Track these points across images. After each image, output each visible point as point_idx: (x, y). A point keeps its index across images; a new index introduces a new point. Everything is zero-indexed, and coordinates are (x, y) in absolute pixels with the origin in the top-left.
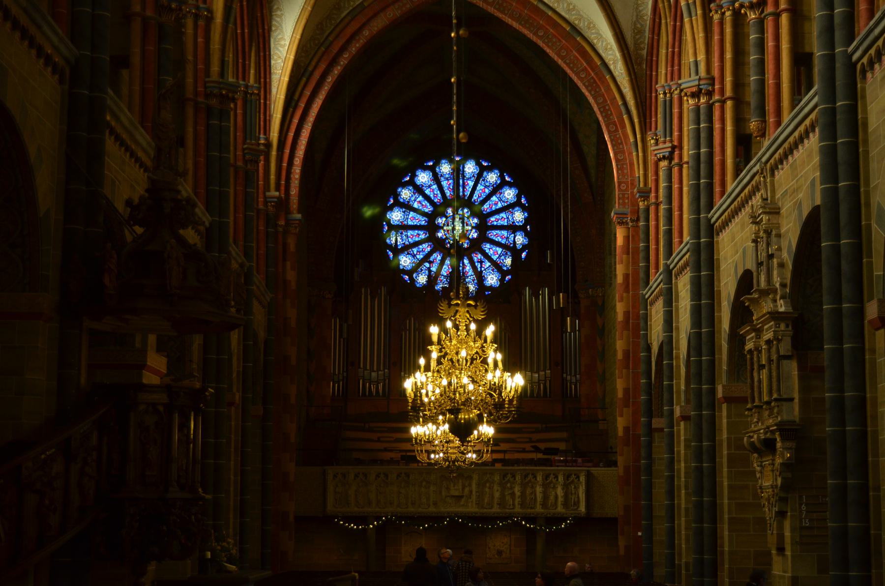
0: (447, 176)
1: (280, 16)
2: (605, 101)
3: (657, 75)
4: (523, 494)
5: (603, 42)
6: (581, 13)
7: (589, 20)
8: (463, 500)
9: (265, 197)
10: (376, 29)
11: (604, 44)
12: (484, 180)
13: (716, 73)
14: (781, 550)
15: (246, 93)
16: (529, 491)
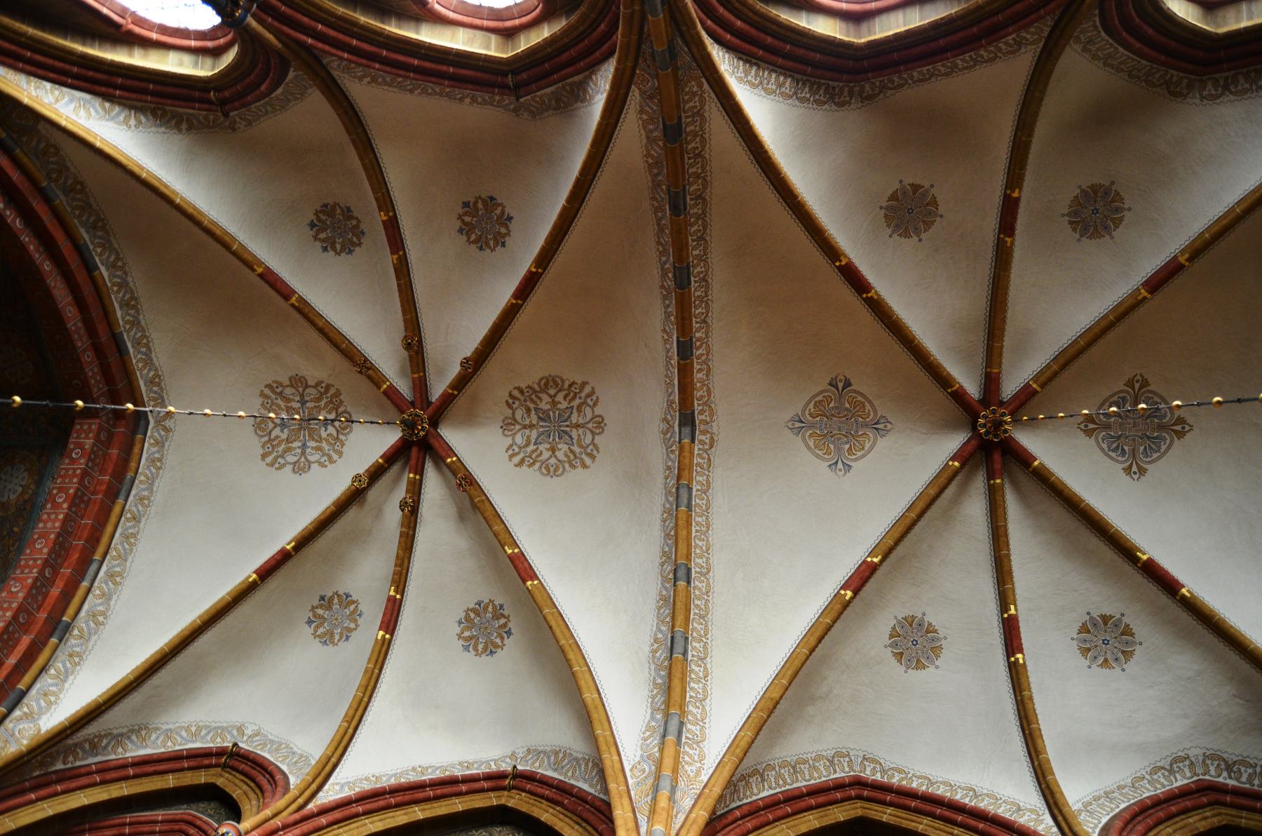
1: (126, 122)
3: (31, 802)
5: (56, 685)
6: (94, 638)
7: (84, 653)
10: (53, 284)
11: (54, 689)
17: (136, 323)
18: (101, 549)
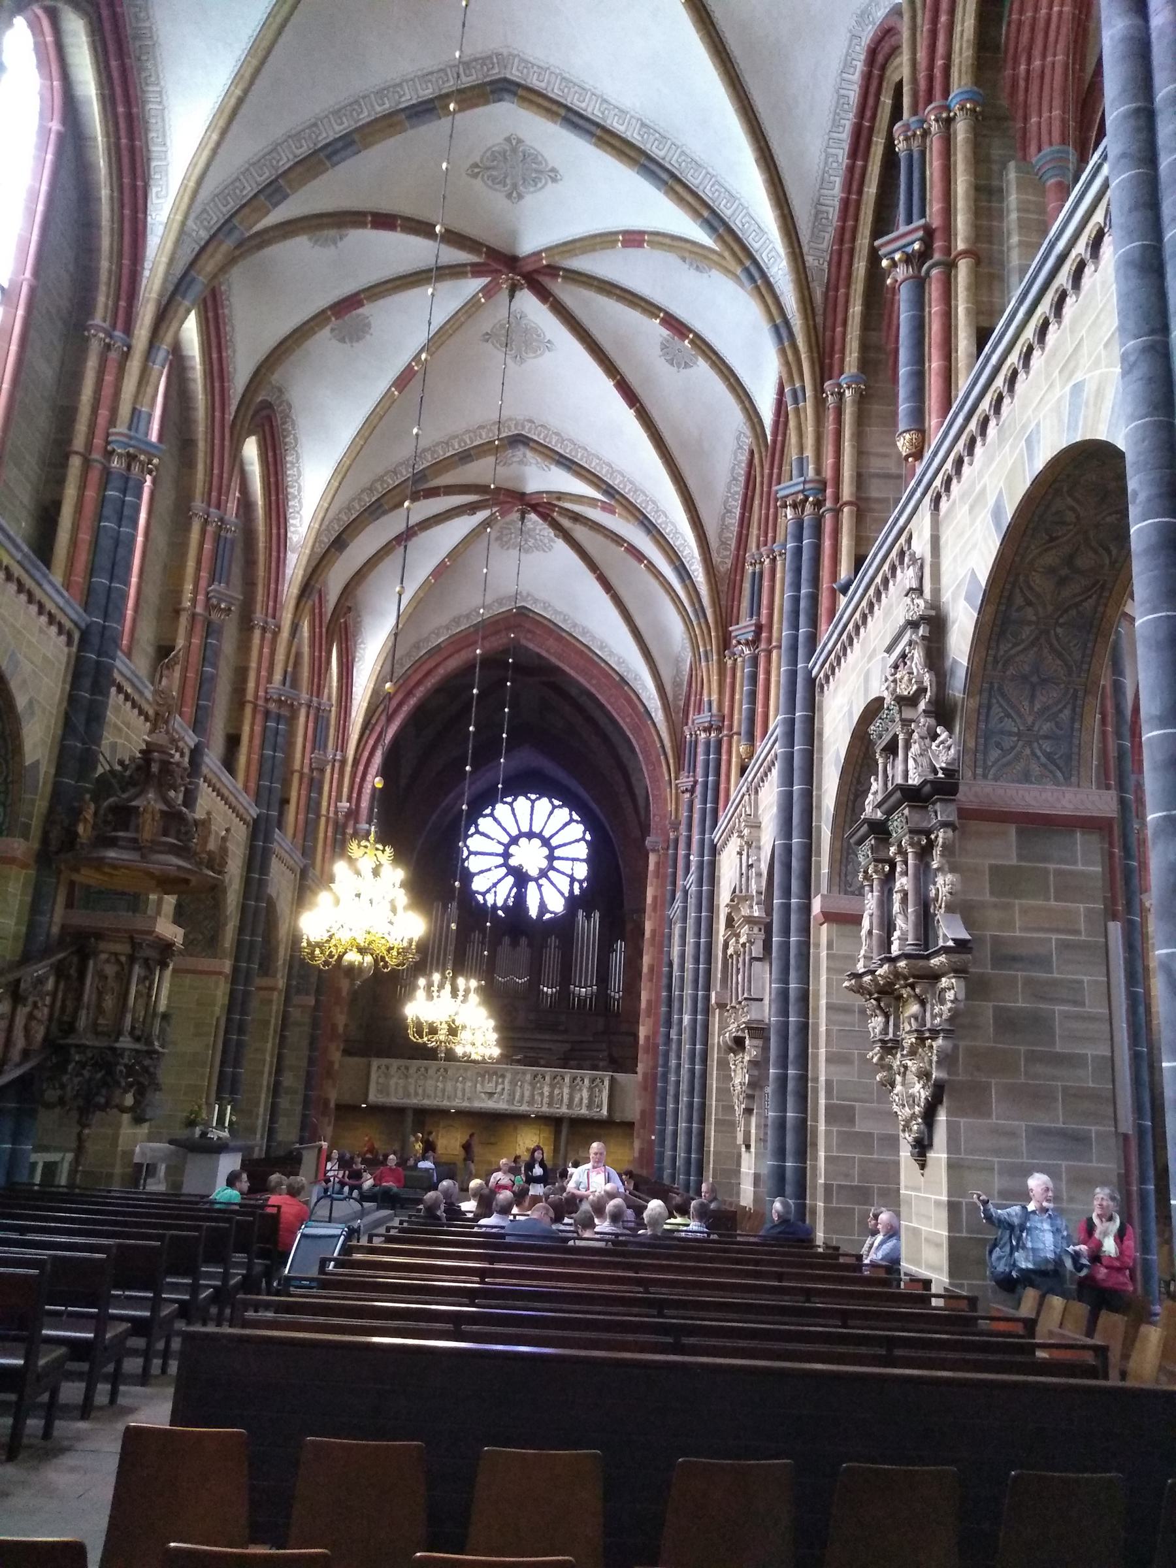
2: (646, 743)
9: (336, 807)
13: (726, 711)
14: (748, 1147)
15: (318, 709)
16: (556, 1092)
17: (468, 616)
18: (586, 651)
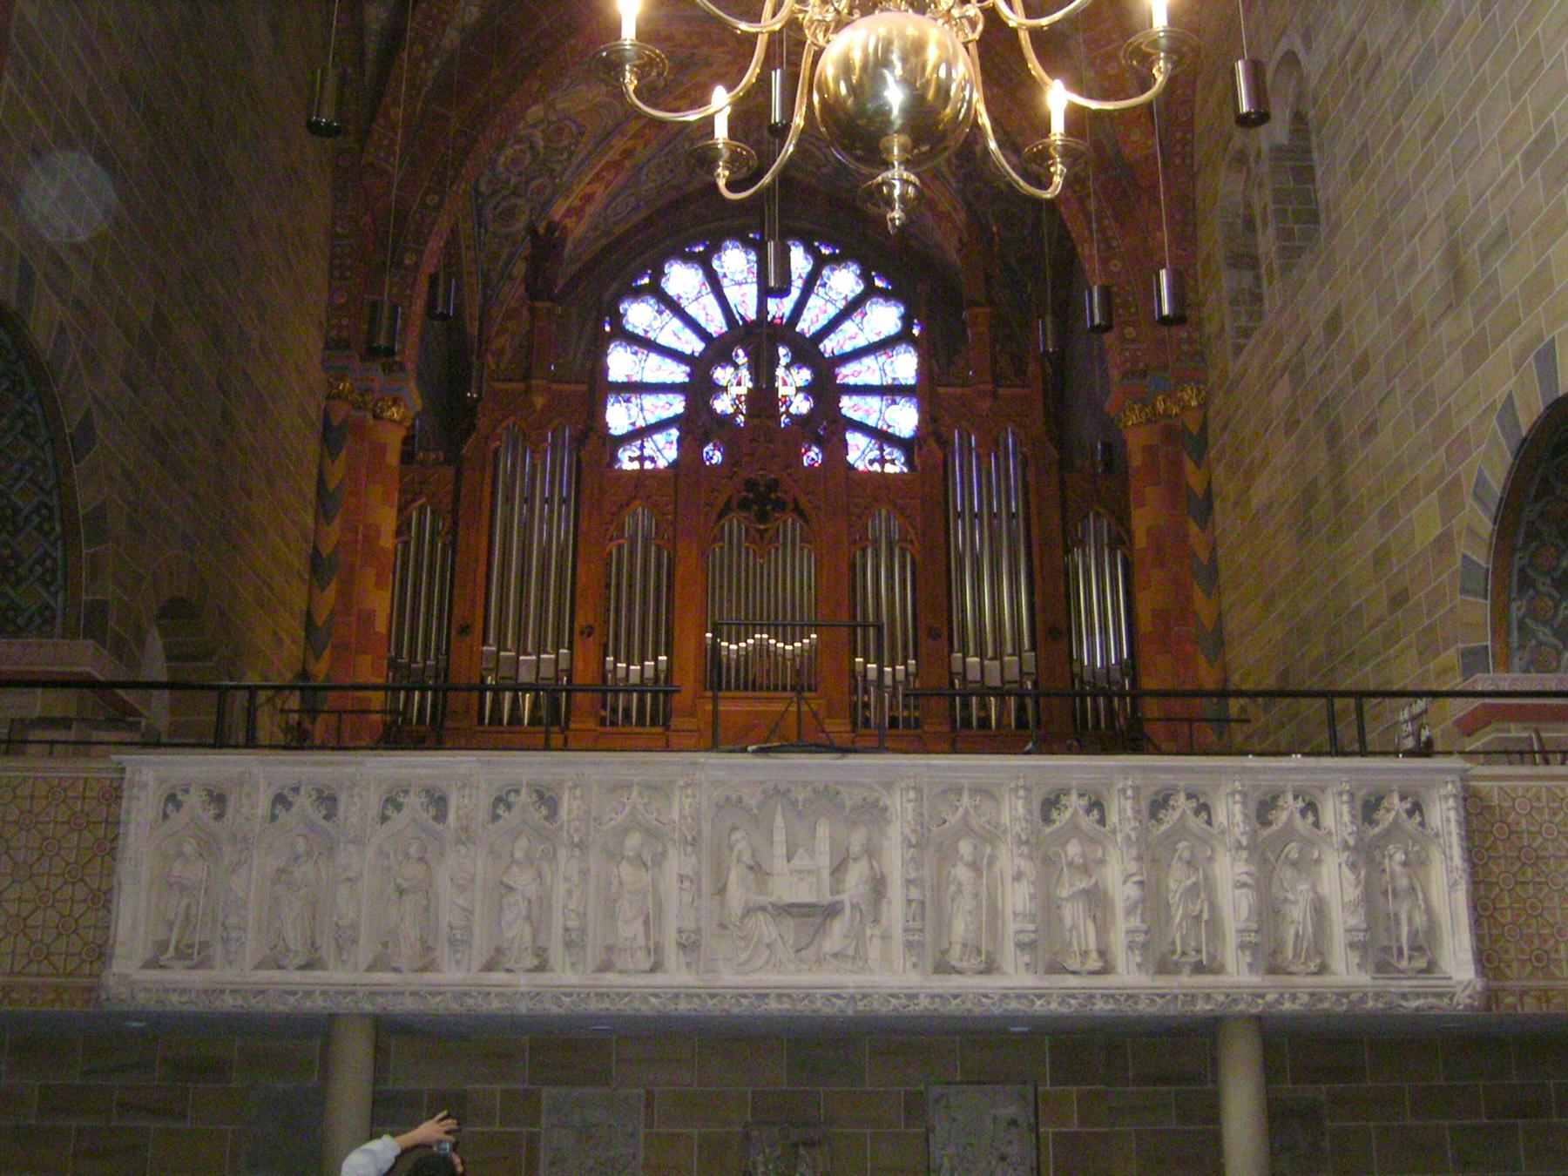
0: (739, 277)
4: (1152, 899)
8: (838, 926)
12: (824, 285)
